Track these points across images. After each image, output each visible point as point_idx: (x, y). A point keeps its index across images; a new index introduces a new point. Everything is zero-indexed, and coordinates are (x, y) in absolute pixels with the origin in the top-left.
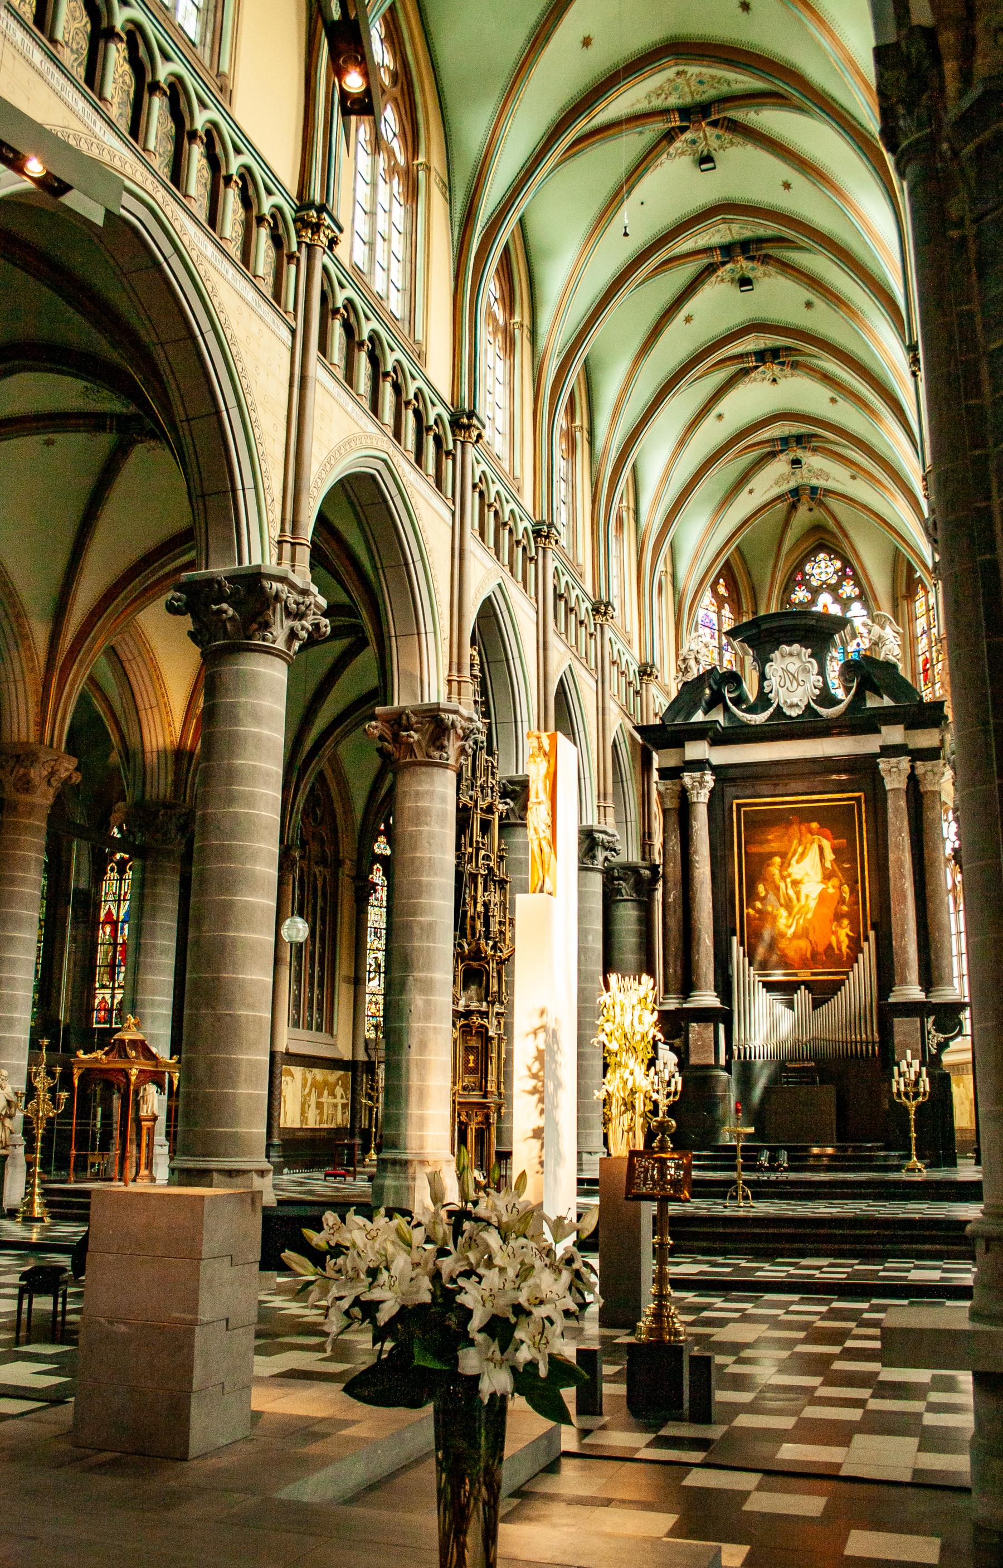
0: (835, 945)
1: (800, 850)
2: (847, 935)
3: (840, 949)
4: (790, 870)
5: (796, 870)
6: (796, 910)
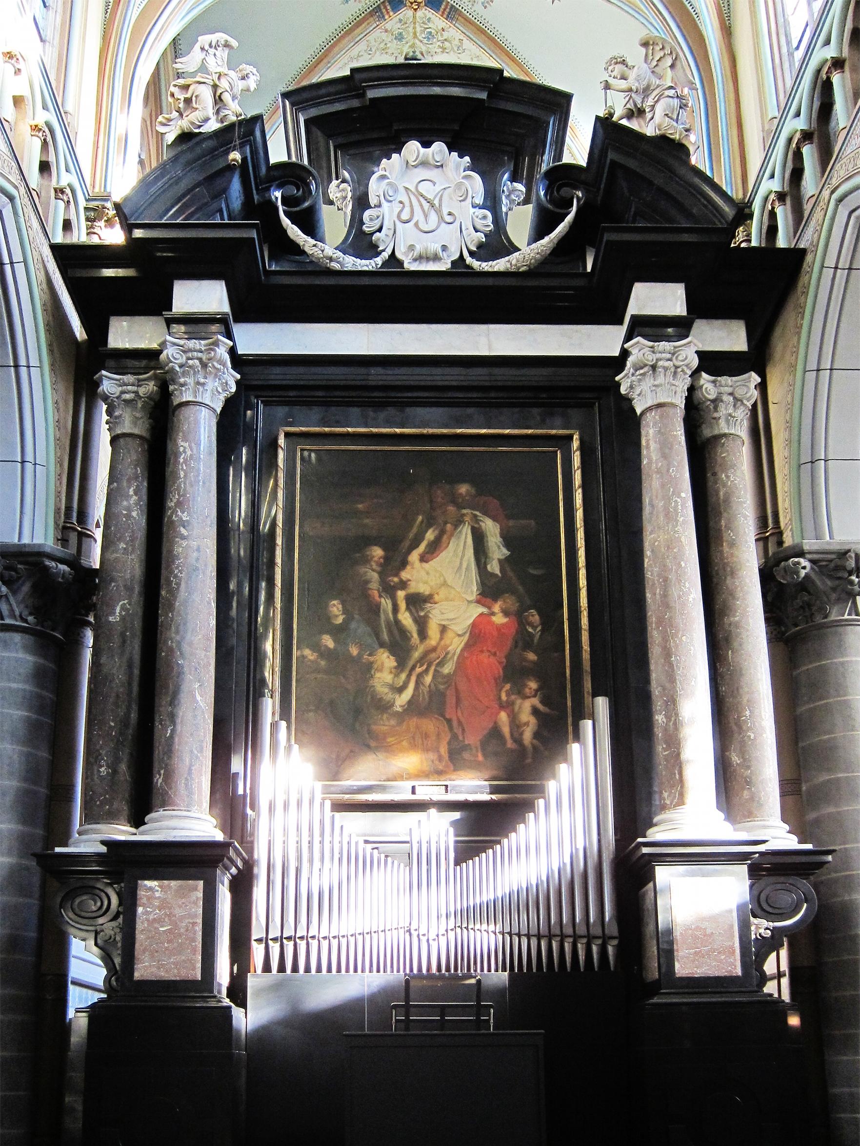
0: (506, 730)
1: (430, 535)
2: (535, 711)
3: (518, 740)
4: (405, 575)
5: (419, 575)
6: (416, 655)
